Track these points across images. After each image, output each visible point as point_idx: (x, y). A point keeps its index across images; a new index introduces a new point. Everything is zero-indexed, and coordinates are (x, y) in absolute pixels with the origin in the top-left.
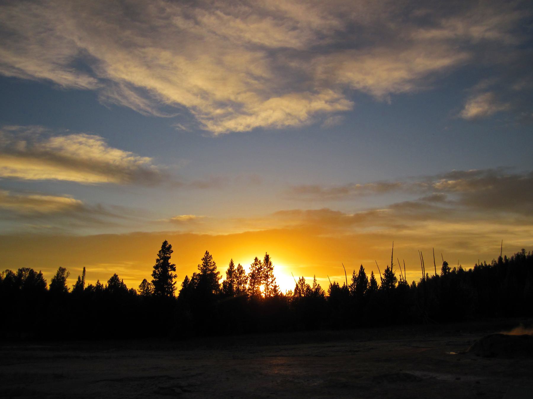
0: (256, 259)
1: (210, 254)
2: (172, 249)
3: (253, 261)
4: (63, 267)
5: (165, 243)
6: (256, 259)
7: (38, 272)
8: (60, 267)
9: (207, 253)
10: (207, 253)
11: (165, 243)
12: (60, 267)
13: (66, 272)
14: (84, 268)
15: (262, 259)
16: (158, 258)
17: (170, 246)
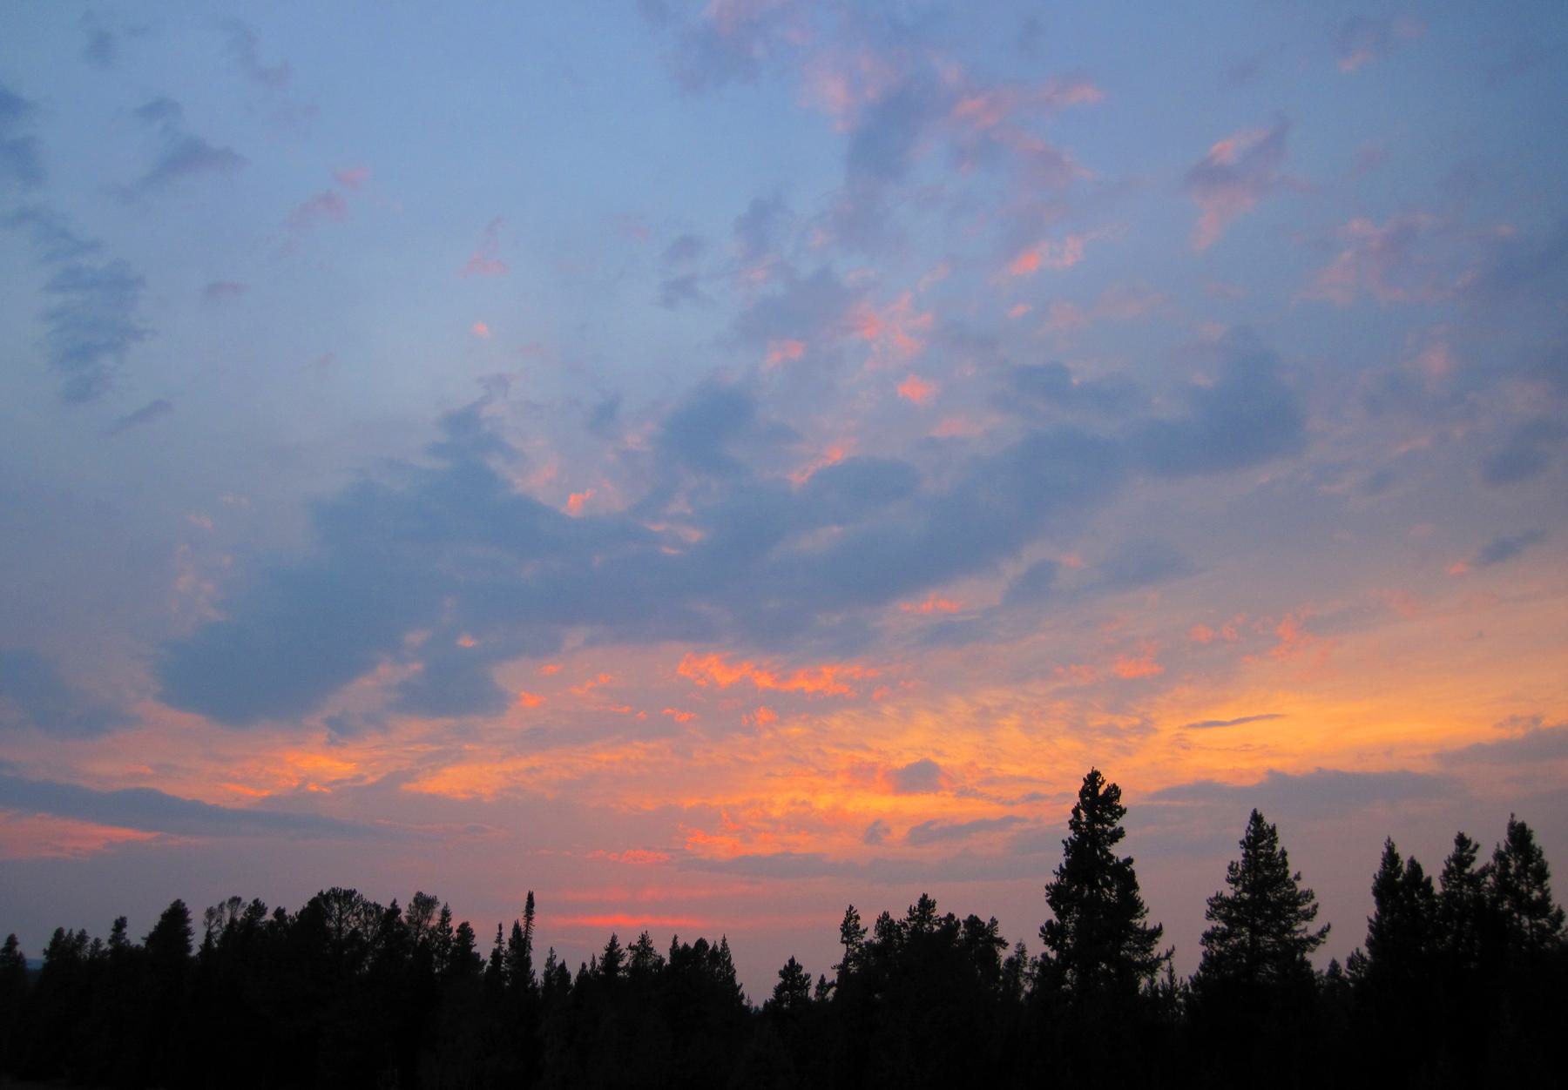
0: (1462, 841)
1: (1269, 820)
2: (1123, 802)
3: (1451, 849)
4: (428, 893)
5: (1093, 779)
6: (1462, 841)
7: (386, 905)
8: (420, 894)
9: (1257, 818)
10: (1257, 818)
11: (1093, 779)
12: (420, 894)
13: (439, 909)
14: (530, 897)
15: (1489, 844)
16: (1071, 833)
17: (1114, 791)
